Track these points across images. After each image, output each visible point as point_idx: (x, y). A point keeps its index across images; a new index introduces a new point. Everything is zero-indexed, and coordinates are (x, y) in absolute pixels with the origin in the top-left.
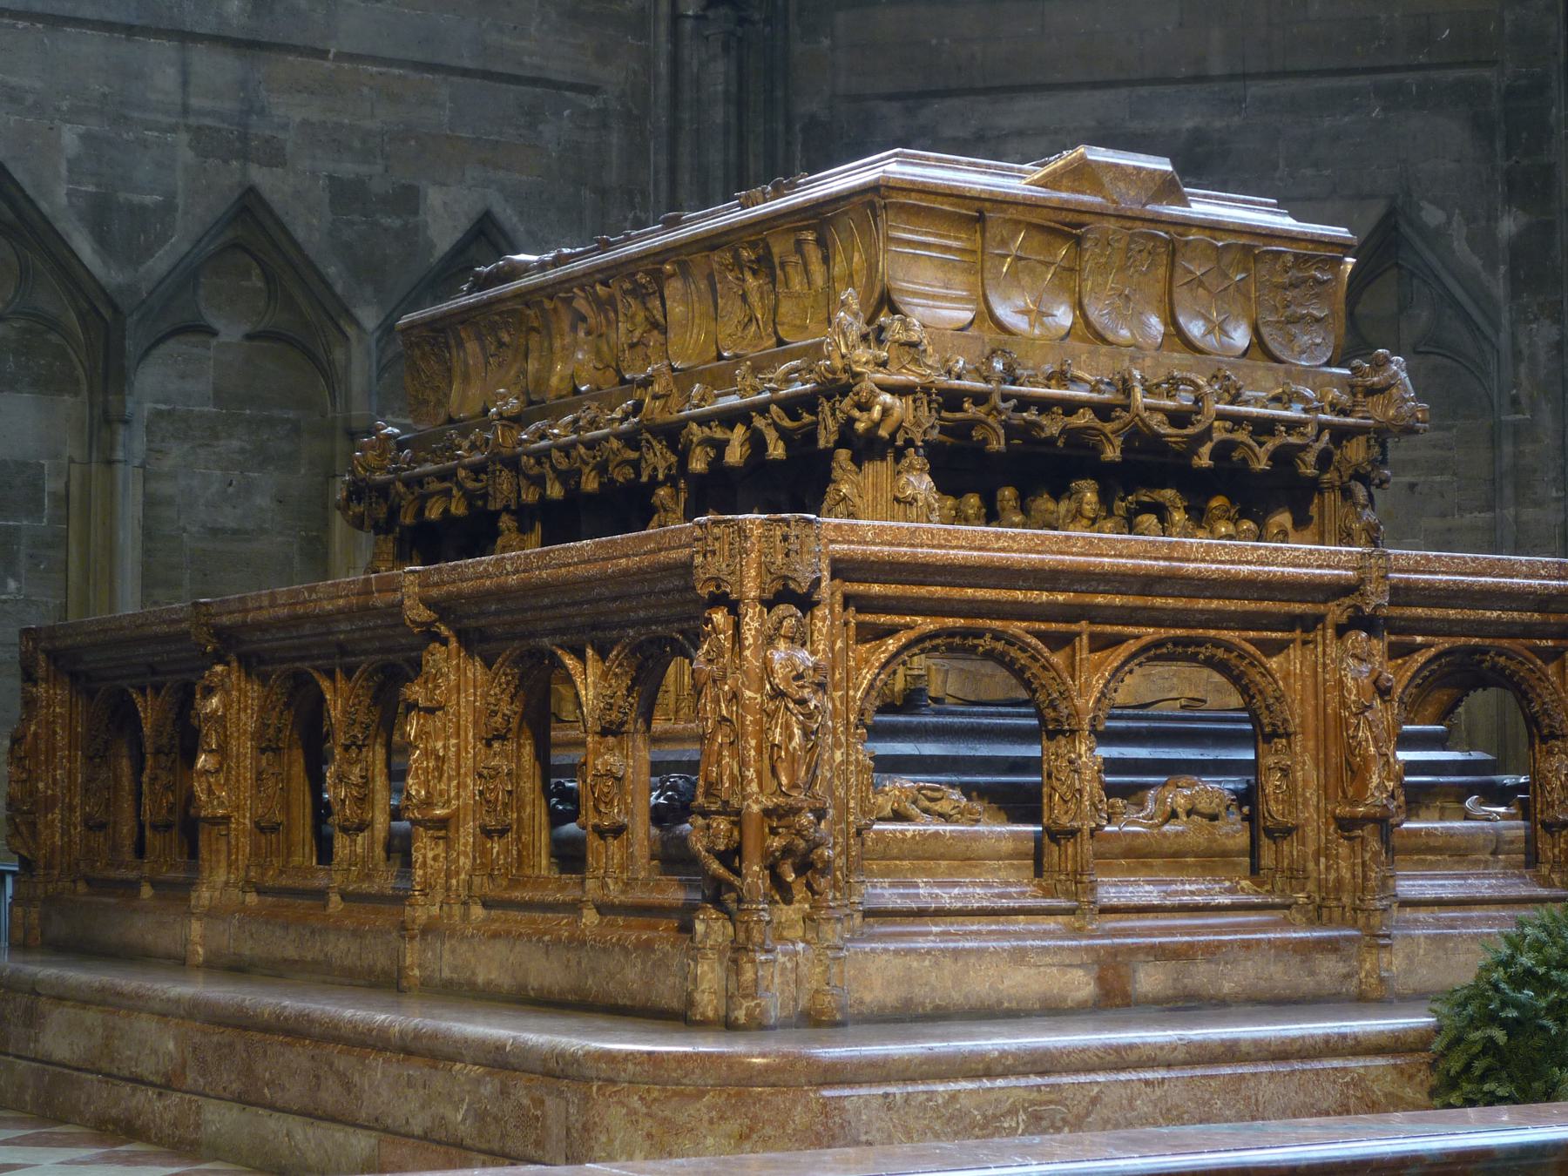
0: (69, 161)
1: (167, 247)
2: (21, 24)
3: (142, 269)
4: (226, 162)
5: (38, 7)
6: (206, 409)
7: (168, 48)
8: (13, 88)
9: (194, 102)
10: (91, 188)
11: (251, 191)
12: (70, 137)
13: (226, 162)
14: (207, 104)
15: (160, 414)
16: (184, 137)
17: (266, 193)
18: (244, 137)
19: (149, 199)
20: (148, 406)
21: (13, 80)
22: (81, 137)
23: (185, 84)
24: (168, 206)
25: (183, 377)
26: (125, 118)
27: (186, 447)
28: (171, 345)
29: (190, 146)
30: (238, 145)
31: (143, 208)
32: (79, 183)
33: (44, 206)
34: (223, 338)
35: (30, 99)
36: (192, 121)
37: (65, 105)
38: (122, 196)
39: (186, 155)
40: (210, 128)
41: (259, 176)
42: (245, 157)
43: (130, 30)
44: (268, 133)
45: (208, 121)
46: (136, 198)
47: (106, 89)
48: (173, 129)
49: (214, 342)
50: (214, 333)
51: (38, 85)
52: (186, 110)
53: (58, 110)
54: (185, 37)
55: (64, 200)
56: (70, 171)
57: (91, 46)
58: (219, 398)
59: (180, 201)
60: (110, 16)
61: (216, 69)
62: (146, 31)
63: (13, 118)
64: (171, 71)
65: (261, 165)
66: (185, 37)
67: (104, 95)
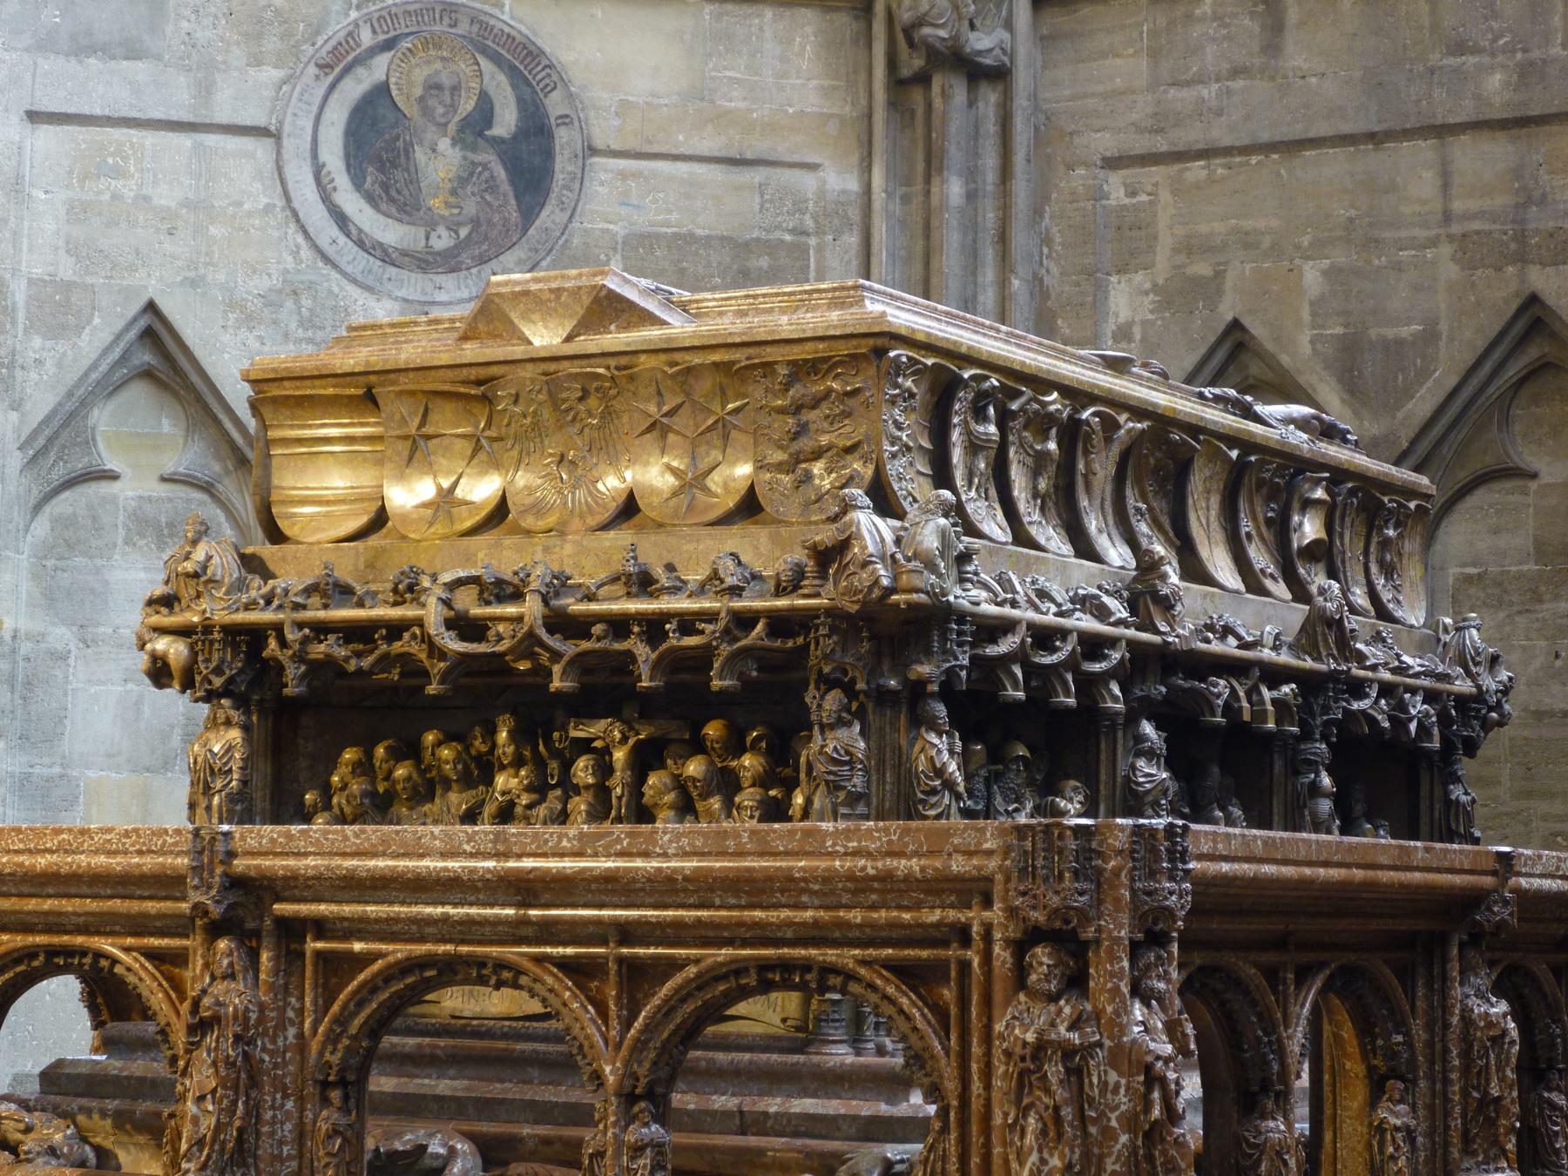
0: (1312, 303)
1: (1429, 383)
2: (1254, 160)
3: (1400, 415)
4: (1499, 269)
5: (1265, 136)
6: (1525, 568)
7: (1425, 148)
8: (1247, 233)
9: (1457, 206)
10: (1339, 330)
11: (1533, 300)
12: (1312, 276)
13: (1499, 269)
14: (1473, 205)
15: (1468, 579)
16: (1446, 250)
17: (1551, 300)
18: (1521, 237)
19: (1405, 332)
20: (1453, 571)
21: (1247, 224)
22: (1325, 273)
23: (1446, 186)
24: (1430, 335)
25: (1496, 532)
26: (1376, 241)
27: (1502, 615)
28: (1479, 497)
29: (1453, 259)
30: (1513, 246)
31: (1399, 342)
32: (1323, 327)
33: (1285, 360)
34: (1545, 478)
35: (1266, 242)
36: (1456, 229)
37: (1306, 241)
38: (1373, 333)
39: (1450, 271)
40: (1478, 233)
41: (1542, 280)
42: (1521, 258)
43: (1372, 137)
44: (1551, 224)
45: (1476, 225)
46: (1390, 333)
47: (1353, 213)
48: (1433, 242)
49: (1533, 485)
50: (1534, 476)
51: (1275, 223)
52: (1447, 217)
53: (1298, 247)
54: (1442, 131)
55: (1306, 349)
56: (1314, 314)
57: (1334, 166)
58: (1541, 551)
59: (1443, 327)
60: (1347, 128)
61: (1483, 161)
62: (1390, 135)
63: (1248, 267)
64: (1428, 175)
65: (1543, 264)
66: (1442, 131)
67: (1351, 220)
